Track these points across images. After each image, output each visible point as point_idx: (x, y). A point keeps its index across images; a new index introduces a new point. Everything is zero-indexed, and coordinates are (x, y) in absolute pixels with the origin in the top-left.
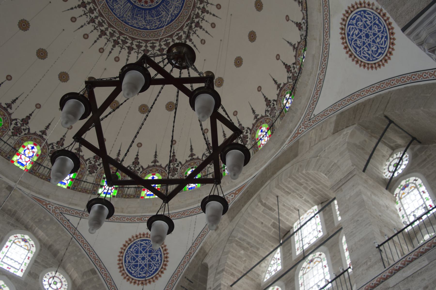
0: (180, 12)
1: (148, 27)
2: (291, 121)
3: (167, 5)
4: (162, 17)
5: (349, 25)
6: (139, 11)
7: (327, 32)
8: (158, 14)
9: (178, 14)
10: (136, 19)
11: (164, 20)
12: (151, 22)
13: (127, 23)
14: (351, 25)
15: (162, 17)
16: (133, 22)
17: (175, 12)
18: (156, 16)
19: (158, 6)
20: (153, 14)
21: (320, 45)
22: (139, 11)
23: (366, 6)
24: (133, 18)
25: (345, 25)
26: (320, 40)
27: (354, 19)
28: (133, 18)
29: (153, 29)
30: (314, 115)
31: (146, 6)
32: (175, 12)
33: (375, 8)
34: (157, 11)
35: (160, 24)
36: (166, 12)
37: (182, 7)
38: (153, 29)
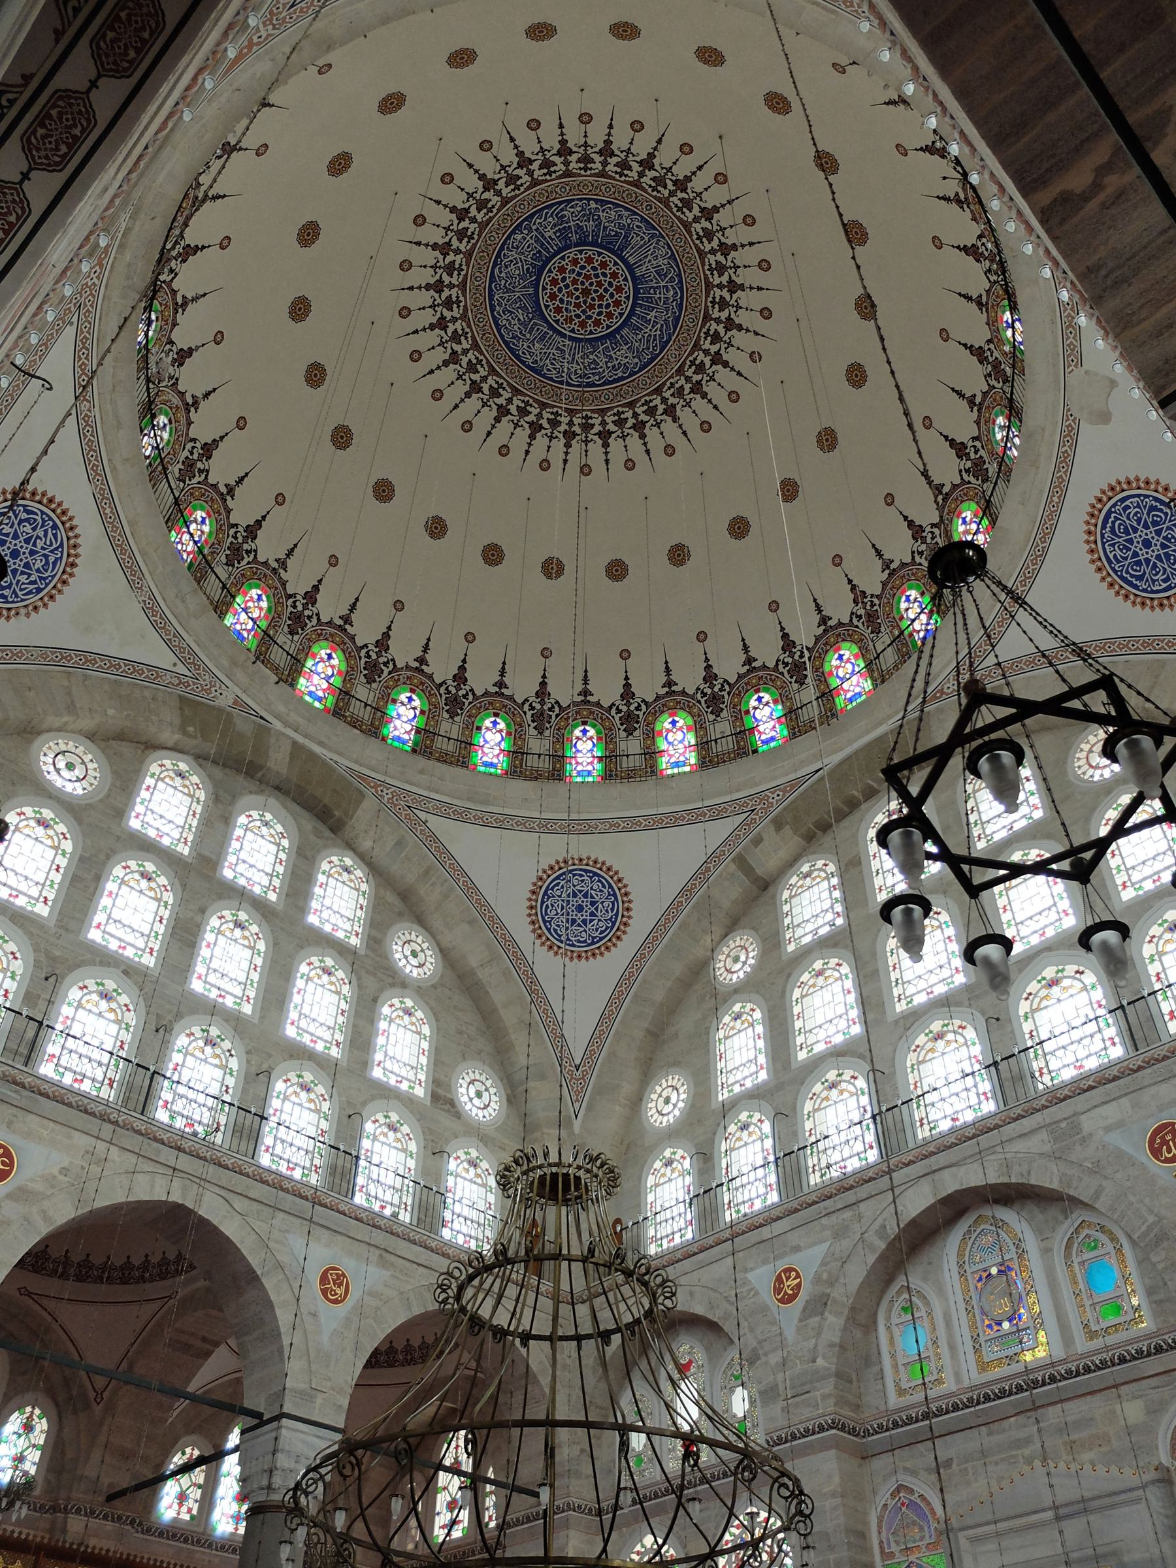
0: (509, 237)
1: (593, 205)
2: (129, 265)
3: (539, 252)
4: (555, 225)
5: (61, 545)
6: (610, 243)
7: (104, 500)
8: (563, 233)
9: (513, 232)
10: (620, 226)
11: (550, 219)
12: (584, 215)
13: (643, 220)
14: (56, 549)
15: (555, 225)
16: (629, 221)
17: (519, 237)
18: (570, 227)
19: (560, 250)
20: (576, 233)
21: (110, 460)
22: (610, 243)
23: (40, 603)
24: (629, 229)
25: (68, 539)
26: (114, 469)
27: (54, 564)
28: (629, 229)
29: (580, 200)
30: (72, 324)
31: (590, 251)
32: (519, 237)
33: (23, 611)
34: (566, 238)
35: (562, 210)
36: (543, 236)
37: (502, 248)
38: (580, 200)
